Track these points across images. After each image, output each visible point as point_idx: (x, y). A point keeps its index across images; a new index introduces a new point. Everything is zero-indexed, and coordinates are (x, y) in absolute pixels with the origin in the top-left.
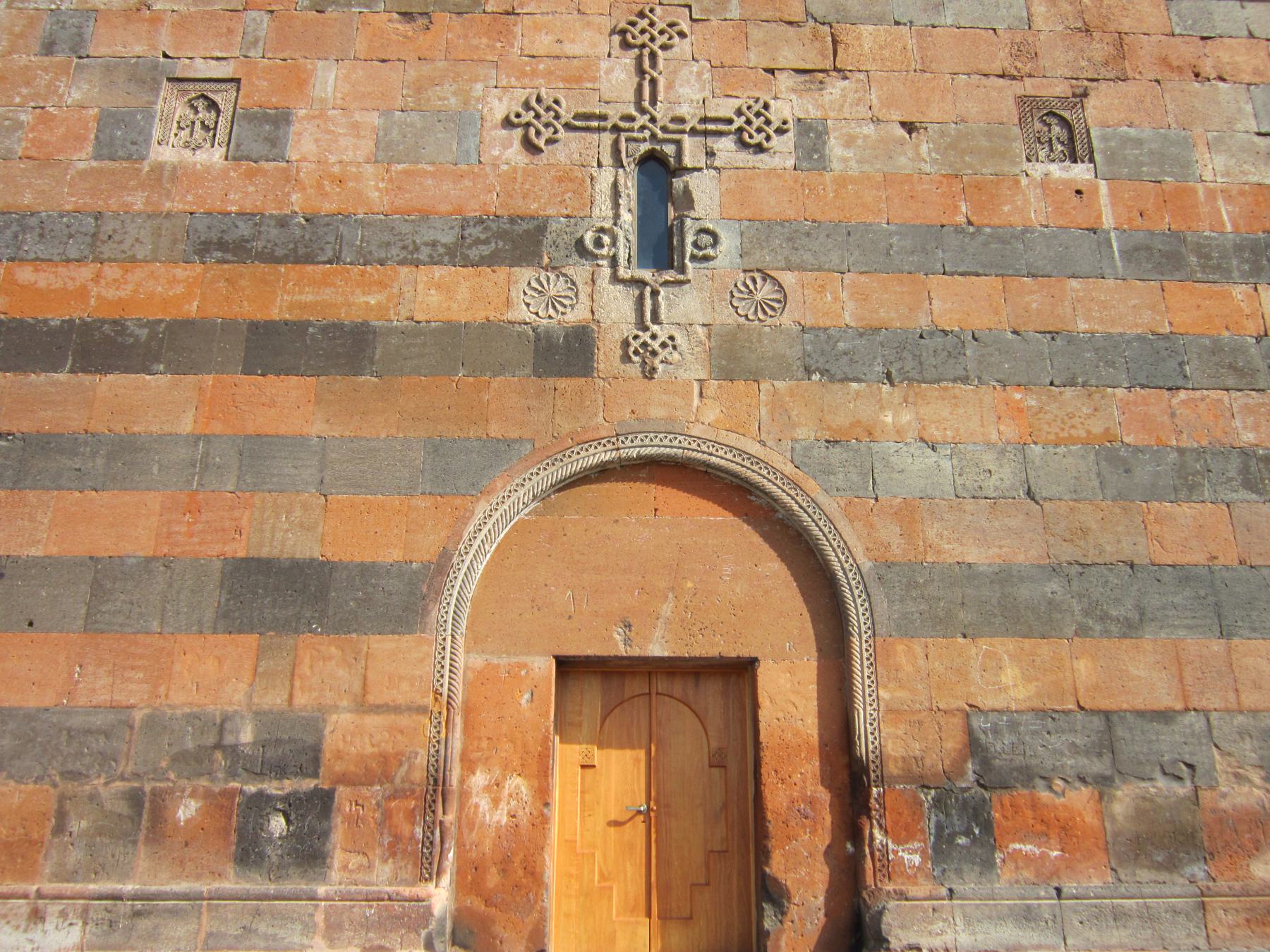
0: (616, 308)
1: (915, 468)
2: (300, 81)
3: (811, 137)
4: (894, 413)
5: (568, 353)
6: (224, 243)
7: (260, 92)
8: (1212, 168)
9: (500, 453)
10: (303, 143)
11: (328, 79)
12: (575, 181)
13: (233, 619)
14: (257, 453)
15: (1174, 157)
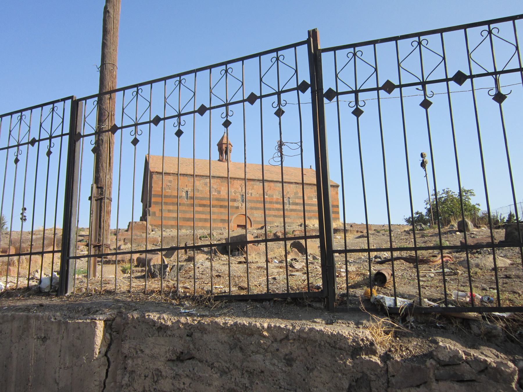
0: (240, 205)
1: (256, 215)
2: (221, 188)
3: (251, 194)
4: (255, 212)
5: (237, 208)
6: (218, 200)
7: (218, 189)
8: (274, 197)
9: (234, 214)
10: (222, 193)
11: (223, 188)
12: (237, 196)
13: (221, 222)
14: (221, 213)
15: (272, 196)
